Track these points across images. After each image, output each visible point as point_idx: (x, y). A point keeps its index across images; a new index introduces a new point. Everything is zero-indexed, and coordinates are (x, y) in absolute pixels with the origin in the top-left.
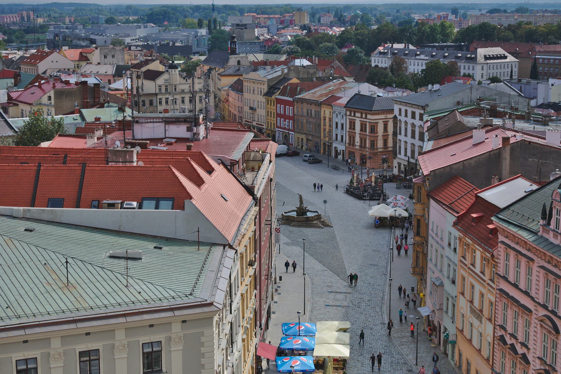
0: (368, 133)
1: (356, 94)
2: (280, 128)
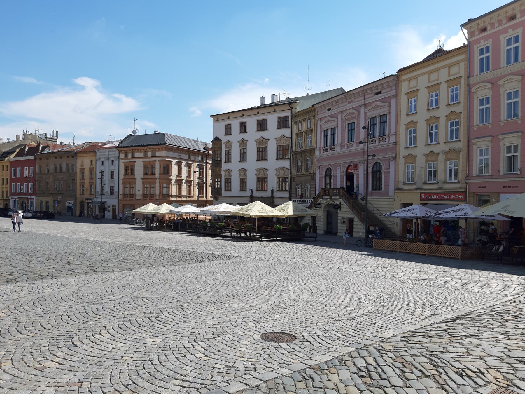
0: (157, 175)
1: (130, 135)
2: (16, 194)
